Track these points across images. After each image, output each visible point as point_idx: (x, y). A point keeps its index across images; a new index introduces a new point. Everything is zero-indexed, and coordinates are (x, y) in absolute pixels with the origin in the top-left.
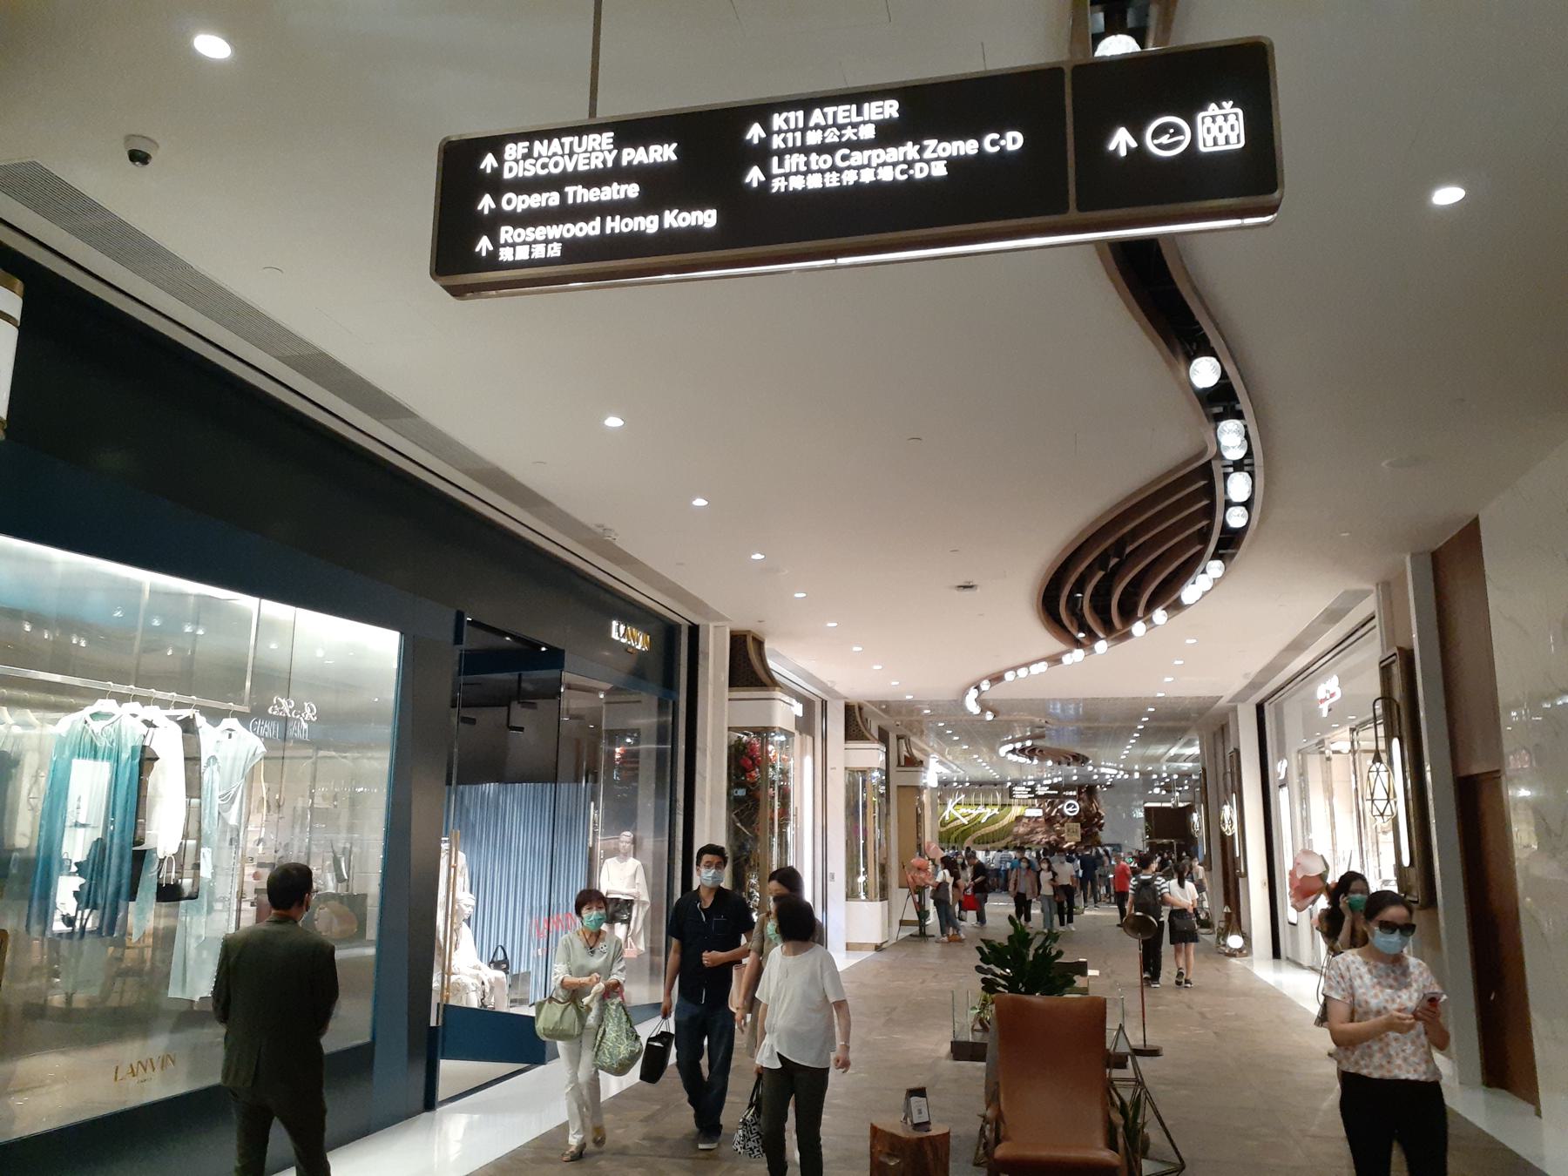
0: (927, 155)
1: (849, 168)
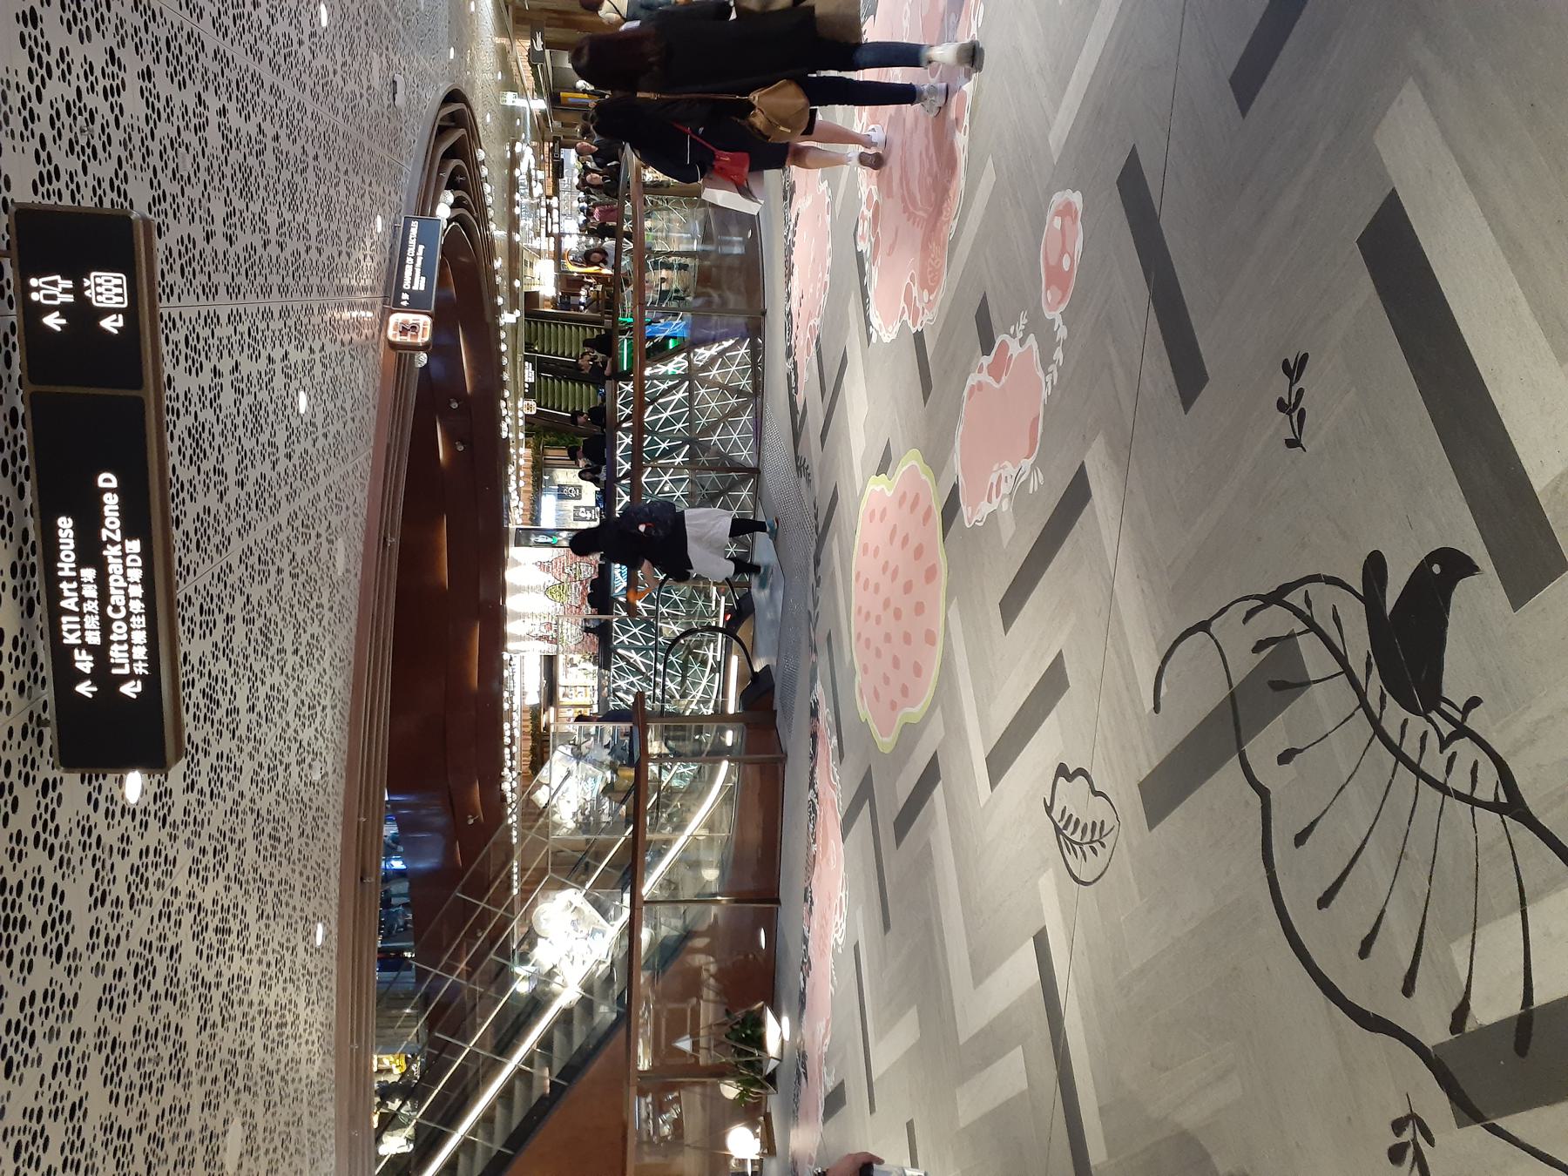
1: (127, 606)
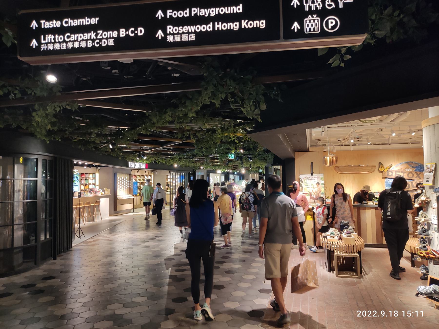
0: (99, 37)
1: (70, 41)
